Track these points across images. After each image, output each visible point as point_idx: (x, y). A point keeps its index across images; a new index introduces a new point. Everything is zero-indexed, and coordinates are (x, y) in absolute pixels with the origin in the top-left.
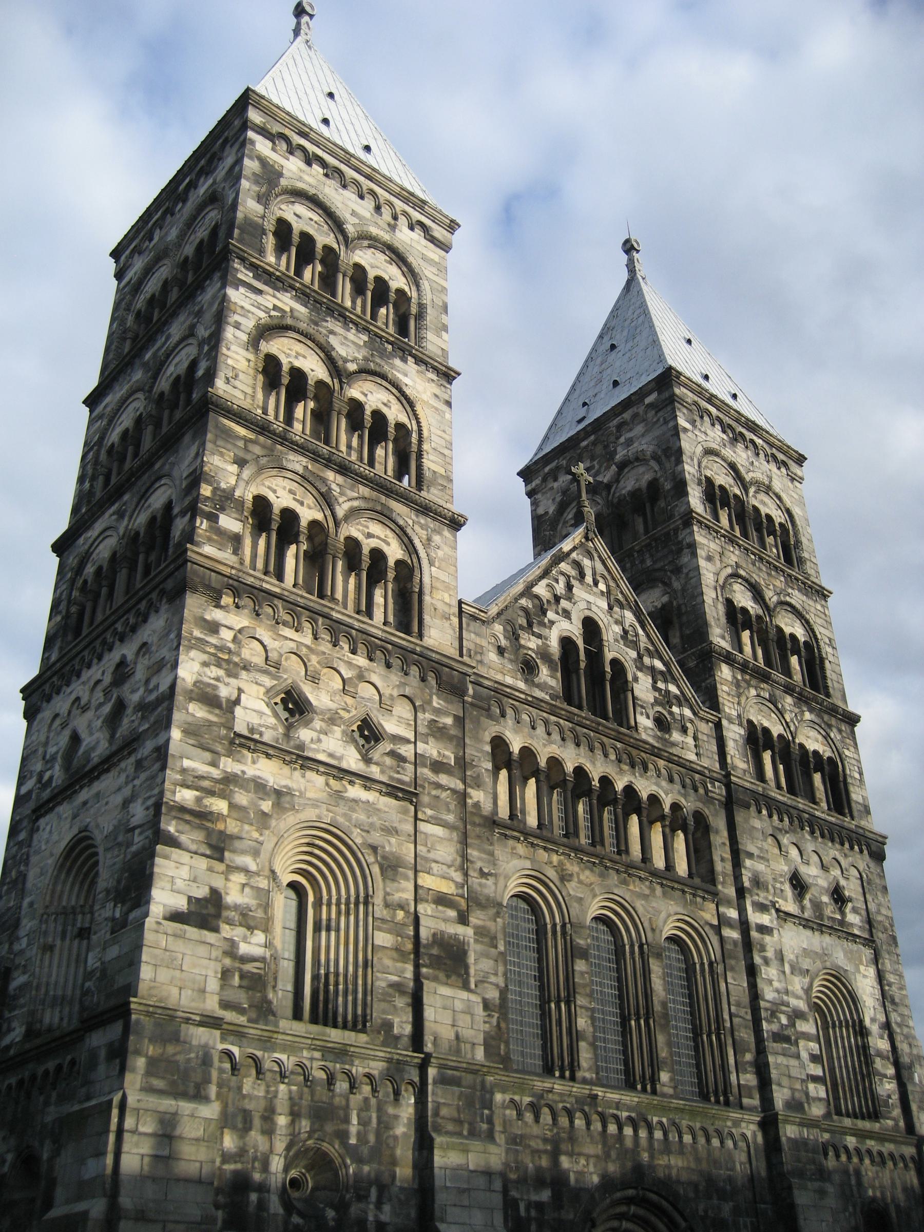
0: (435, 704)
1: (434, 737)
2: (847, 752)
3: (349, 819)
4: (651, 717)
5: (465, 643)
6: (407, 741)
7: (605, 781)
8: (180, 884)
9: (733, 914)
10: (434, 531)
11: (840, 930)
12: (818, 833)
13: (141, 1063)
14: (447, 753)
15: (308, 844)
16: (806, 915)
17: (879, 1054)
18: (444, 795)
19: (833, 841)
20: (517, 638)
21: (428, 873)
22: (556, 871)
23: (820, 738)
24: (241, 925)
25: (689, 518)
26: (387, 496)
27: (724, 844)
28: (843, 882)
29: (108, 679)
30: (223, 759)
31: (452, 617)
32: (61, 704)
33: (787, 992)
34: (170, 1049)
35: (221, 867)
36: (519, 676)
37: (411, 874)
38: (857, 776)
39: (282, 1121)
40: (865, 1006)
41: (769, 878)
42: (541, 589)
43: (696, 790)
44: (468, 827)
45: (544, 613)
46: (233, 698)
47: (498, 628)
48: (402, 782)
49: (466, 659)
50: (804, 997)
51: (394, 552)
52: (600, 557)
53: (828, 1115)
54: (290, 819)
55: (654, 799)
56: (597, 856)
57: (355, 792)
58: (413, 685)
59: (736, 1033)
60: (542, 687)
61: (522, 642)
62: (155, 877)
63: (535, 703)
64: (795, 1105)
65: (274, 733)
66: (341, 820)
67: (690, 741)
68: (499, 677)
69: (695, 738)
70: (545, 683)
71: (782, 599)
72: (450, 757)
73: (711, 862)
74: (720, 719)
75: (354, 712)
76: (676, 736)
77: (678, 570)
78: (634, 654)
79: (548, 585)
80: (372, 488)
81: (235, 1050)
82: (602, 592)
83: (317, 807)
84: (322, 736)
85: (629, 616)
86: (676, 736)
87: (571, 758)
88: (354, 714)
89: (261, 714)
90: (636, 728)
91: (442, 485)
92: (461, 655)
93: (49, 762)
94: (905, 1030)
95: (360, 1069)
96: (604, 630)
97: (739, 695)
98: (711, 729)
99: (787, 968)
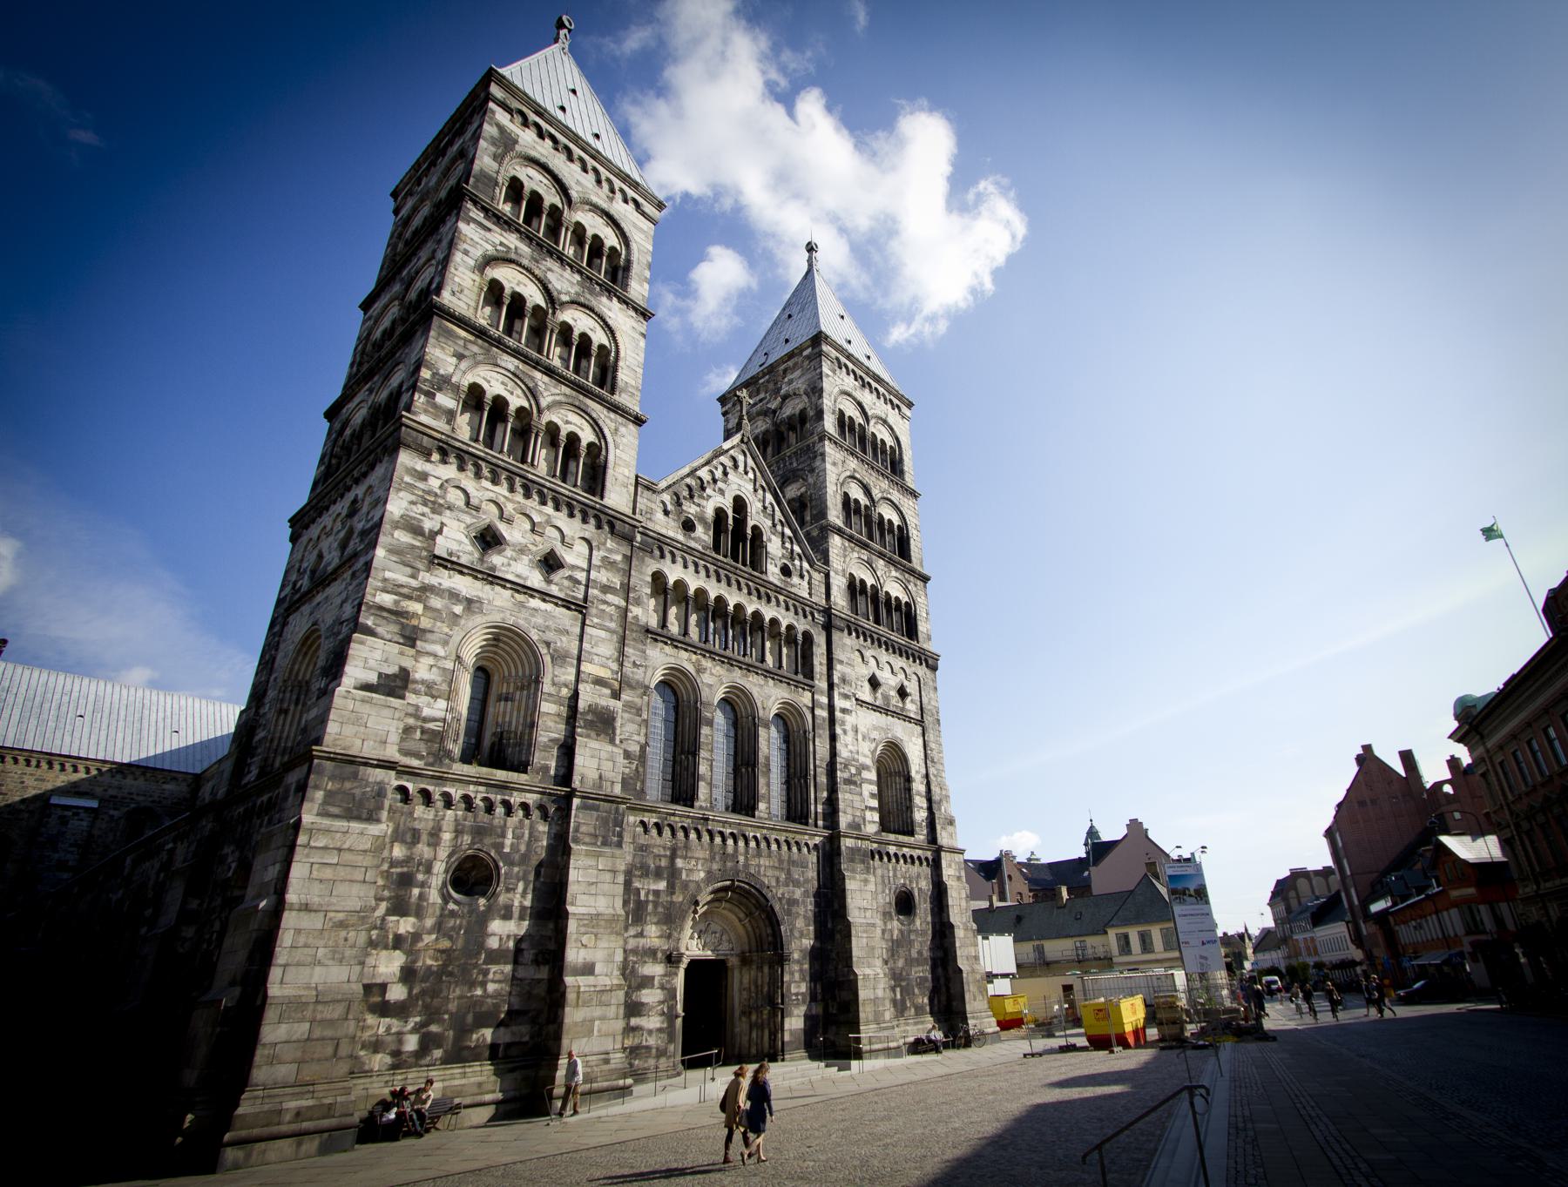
3: (529, 624)
5: (638, 505)
6: (583, 570)
7: (739, 607)
9: (824, 700)
11: (901, 715)
12: (891, 651)
13: (319, 795)
16: (877, 704)
17: (919, 794)
18: (608, 609)
19: (901, 655)
24: (426, 694)
25: (823, 436)
28: (906, 683)
29: (345, 512)
30: (421, 573)
32: (314, 531)
33: (858, 753)
34: (348, 785)
35: (412, 652)
37: (575, 662)
39: (447, 836)
42: (704, 473)
43: (805, 616)
45: (703, 489)
46: (436, 530)
47: (666, 497)
48: (573, 597)
49: (638, 517)
51: (587, 436)
53: (876, 833)
54: (479, 619)
55: (774, 622)
56: (726, 657)
57: (535, 603)
58: (590, 530)
59: (818, 779)
60: (696, 540)
61: (684, 508)
62: (349, 657)
63: (689, 550)
64: (855, 826)
66: (521, 622)
67: (805, 584)
68: (663, 531)
69: (810, 583)
70: (699, 538)
72: (617, 582)
73: (812, 665)
75: (541, 547)
77: (812, 470)
78: (769, 523)
80: (572, 388)
81: (410, 786)
85: (769, 497)
86: (795, 580)
87: (714, 590)
88: (542, 547)
89: (460, 543)
92: (634, 513)
93: (301, 573)
94: (939, 779)
97: (845, 556)
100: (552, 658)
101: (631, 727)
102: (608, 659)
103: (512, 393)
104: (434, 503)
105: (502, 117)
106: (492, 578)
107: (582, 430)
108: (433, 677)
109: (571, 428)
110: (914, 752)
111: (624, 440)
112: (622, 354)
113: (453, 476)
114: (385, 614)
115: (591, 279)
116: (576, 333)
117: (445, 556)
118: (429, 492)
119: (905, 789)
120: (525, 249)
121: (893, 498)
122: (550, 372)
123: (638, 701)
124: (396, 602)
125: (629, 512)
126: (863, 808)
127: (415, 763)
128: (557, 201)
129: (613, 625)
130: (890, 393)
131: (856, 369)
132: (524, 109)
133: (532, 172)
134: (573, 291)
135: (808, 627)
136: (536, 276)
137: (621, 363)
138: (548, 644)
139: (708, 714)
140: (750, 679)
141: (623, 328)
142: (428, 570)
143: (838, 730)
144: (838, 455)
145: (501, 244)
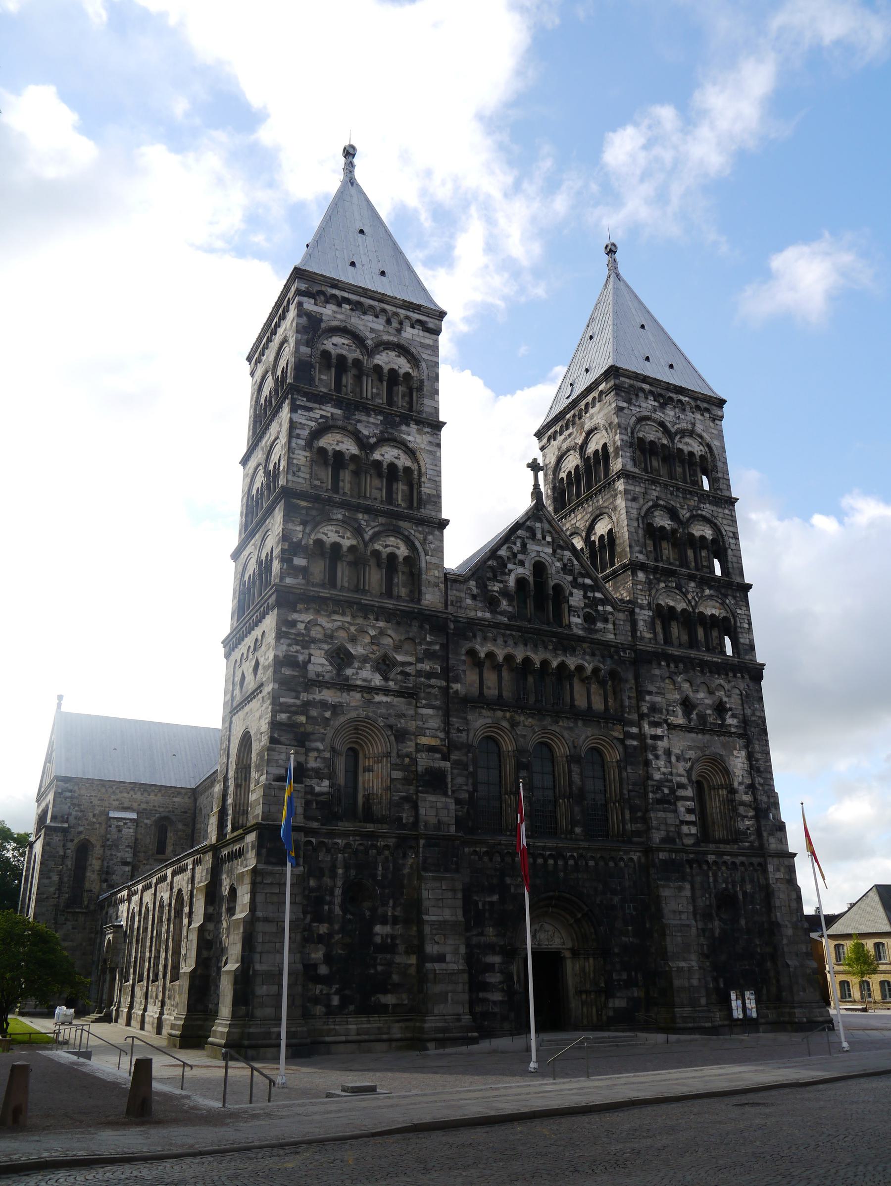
0: (428, 639)
1: (429, 659)
2: (739, 611)
4: (581, 616)
5: (449, 597)
6: (410, 664)
7: (545, 663)
8: (281, 762)
11: (722, 730)
14: (435, 666)
15: (355, 729)
17: (742, 803)
19: (719, 674)
20: (486, 586)
21: (424, 736)
22: (509, 722)
23: (717, 605)
26: (396, 519)
27: (631, 688)
28: (725, 699)
30: (302, 694)
31: (440, 585)
33: (671, 774)
35: (303, 750)
36: (487, 610)
38: (746, 626)
40: (735, 776)
41: (664, 706)
42: (503, 552)
43: (611, 657)
44: (450, 705)
45: (506, 566)
46: (306, 660)
47: (472, 583)
50: (686, 775)
52: (547, 520)
53: (697, 844)
54: (342, 719)
55: (580, 668)
57: (379, 698)
60: (503, 613)
61: (489, 588)
63: (497, 625)
66: (371, 714)
67: (610, 626)
68: (472, 614)
69: (614, 624)
70: (505, 610)
71: (694, 513)
73: (622, 701)
74: (633, 609)
75: (378, 653)
76: (600, 625)
78: (570, 578)
79: (508, 548)
82: (548, 542)
83: (357, 710)
84: (359, 671)
86: (600, 625)
89: (323, 665)
90: (569, 626)
91: (434, 502)
94: (766, 788)
95: (382, 843)
96: (549, 567)
97: (650, 590)
98: (627, 616)
99: (673, 759)
100: (395, 737)
101: (460, 780)
102: (436, 730)
103: (343, 537)
104: (302, 641)
106: (347, 686)
108: (318, 765)
109: (389, 550)
110: (738, 763)
111: (432, 546)
112: (423, 470)
113: (312, 617)
115: (391, 414)
116: (385, 465)
117: (315, 677)
118: (299, 634)
119: (728, 800)
120: (338, 412)
121: (704, 513)
122: (368, 510)
123: (464, 758)
124: (289, 718)
125: (440, 607)
126: (677, 823)
127: (315, 825)
128: (358, 354)
129: (438, 703)
130: (695, 399)
131: (653, 389)
132: (323, 288)
133: (336, 340)
135: (614, 666)
136: (349, 431)
137: (423, 479)
138: (391, 727)
139: (524, 760)
140: (561, 724)
141: (422, 446)
143: (651, 757)
144: (637, 489)
145: (322, 416)
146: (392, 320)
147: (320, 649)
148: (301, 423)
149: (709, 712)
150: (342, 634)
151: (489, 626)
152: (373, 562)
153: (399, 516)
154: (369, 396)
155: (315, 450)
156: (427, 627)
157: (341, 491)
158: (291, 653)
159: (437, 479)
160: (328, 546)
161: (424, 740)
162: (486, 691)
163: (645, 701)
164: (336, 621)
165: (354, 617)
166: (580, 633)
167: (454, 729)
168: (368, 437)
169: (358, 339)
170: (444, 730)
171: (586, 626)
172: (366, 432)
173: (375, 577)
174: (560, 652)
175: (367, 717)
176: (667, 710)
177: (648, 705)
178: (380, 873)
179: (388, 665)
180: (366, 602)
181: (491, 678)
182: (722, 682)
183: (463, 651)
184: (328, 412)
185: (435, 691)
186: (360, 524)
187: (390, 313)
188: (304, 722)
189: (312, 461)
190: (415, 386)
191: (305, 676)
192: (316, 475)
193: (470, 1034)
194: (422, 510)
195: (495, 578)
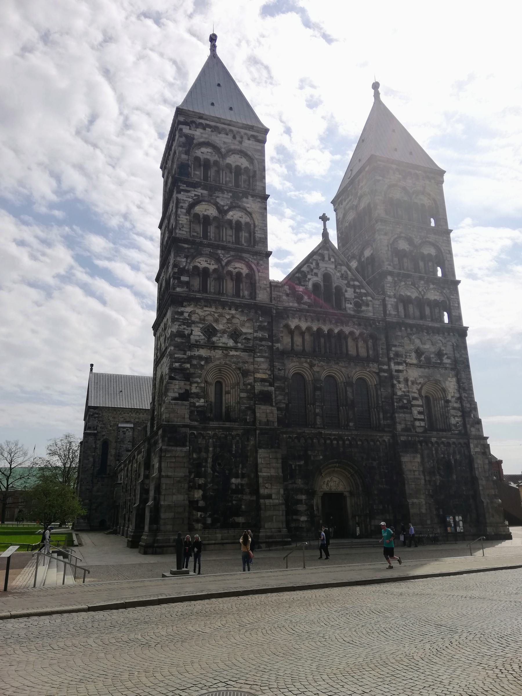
0: (260, 319)
3: (231, 362)
7: (330, 331)
10: (260, 260)
14: (265, 334)
19: (439, 334)
20: (295, 288)
27: (384, 343)
28: (443, 348)
30: (188, 352)
31: (267, 289)
36: (295, 302)
45: (306, 276)
47: (286, 287)
51: (245, 271)
54: (211, 365)
55: (352, 333)
57: (232, 353)
60: (305, 303)
61: (297, 289)
63: (301, 310)
65: (204, 341)
66: (227, 362)
68: (287, 304)
75: (231, 328)
76: (364, 308)
83: (219, 360)
84: (220, 338)
89: (199, 336)
90: (345, 309)
91: (263, 242)
100: (242, 374)
102: (266, 370)
103: (210, 264)
105: (186, 130)
106: (213, 347)
107: (242, 269)
109: (237, 270)
112: (257, 223)
113: (192, 309)
114: (177, 371)
117: (194, 343)
118: (185, 319)
120: (205, 192)
122: (224, 248)
124: (180, 365)
125: (267, 301)
128: (216, 158)
129: (267, 355)
133: (203, 150)
134: (229, 203)
137: (256, 229)
138: (239, 369)
140: (340, 364)
141: (256, 210)
142: (190, 350)
145: (195, 195)
146: (237, 136)
147: (197, 327)
148: (183, 200)
149: (432, 356)
150: (210, 318)
151: (297, 311)
152: (228, 278)
153: (242, 251)
154: (224, 183)
155: (192, 215)
156: (260, 312)
157: (209, 238)
158: (180, 330)
159: (265, 228)
160: (201, 269)
161: (258, 376)
162: (295, 347)
163: (392, 351)
164: (206, 311)
165: (216, 308)
166: (352, 313)
167: (276, 369)
168: (223, 206)
169: (216, 148)
170: (270, 370)
171: (356, 309)
172: (222, 203)
173: (229, 286)
174: (339, 324)
175: (226, 364)
176: (406, 356)
177: (394, 353)
178: (234, 449)
179: (238, 335)
180: (224, 300)
181: (298, 340)
182: (441, 338)
183: (282, 325)
184: (199, 192)
185: (265, 348)
186: (219, 256)
187: (235, 132)
188: (189, 367)
189: (190, 221)
190: (251, 174)
191: (190, 343)
192: (194, 229)
193: (286, 539)
194: (256, 247)
195: (300, 284)
